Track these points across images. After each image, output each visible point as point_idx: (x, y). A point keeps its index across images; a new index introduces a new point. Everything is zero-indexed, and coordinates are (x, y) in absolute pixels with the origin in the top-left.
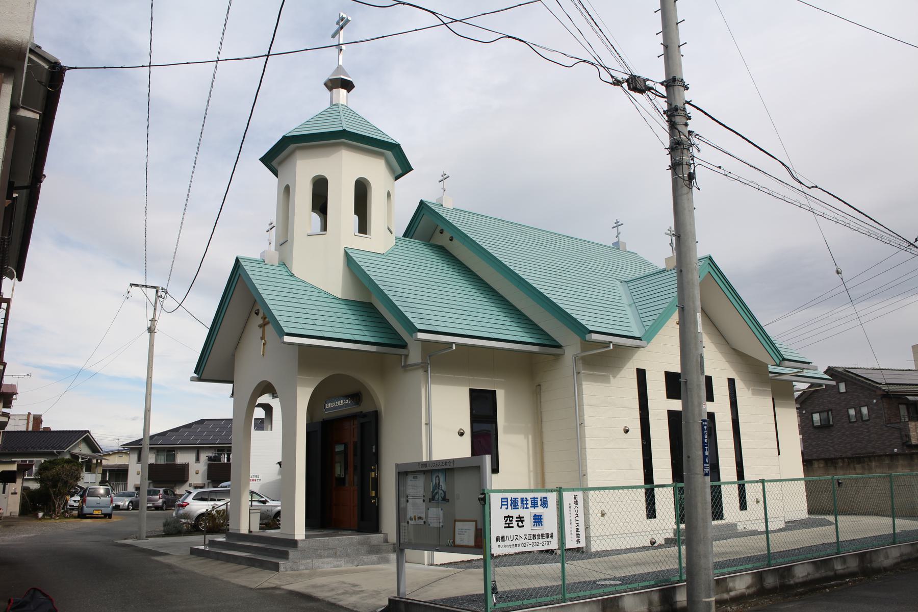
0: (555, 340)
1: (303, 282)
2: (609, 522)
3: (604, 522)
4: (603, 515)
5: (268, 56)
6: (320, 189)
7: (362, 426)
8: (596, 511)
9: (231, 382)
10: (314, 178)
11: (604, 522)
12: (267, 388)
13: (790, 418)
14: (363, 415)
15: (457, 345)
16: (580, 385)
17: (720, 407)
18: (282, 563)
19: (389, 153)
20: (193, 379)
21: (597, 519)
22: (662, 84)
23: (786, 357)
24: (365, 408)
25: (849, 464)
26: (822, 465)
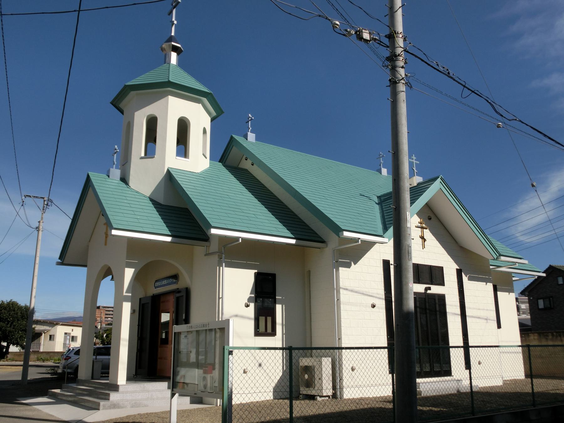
0: (321, 238)
1: (137, 192)
2: (252, 378)
3: (247, 378)
4: (245, 372)
5: (79, 11)
6: (152, 124)
7: (178, 299)
8: (239, 368)
9: (86, 266)
10: (148, 116)
11: (247, 378)
12: (108, 272)
13: (508, 300)
14: (178, 291)
15: (243, 239)
16: (337, 270)
17: (448, 290)
18: (102, 403)
19: (205, 100)
20: (58, 264)
21: (239, 375)
22: (386, 36)
23: (502, 253)
24: (180, 285)
25: (557, 337)
26: (536, 337)
